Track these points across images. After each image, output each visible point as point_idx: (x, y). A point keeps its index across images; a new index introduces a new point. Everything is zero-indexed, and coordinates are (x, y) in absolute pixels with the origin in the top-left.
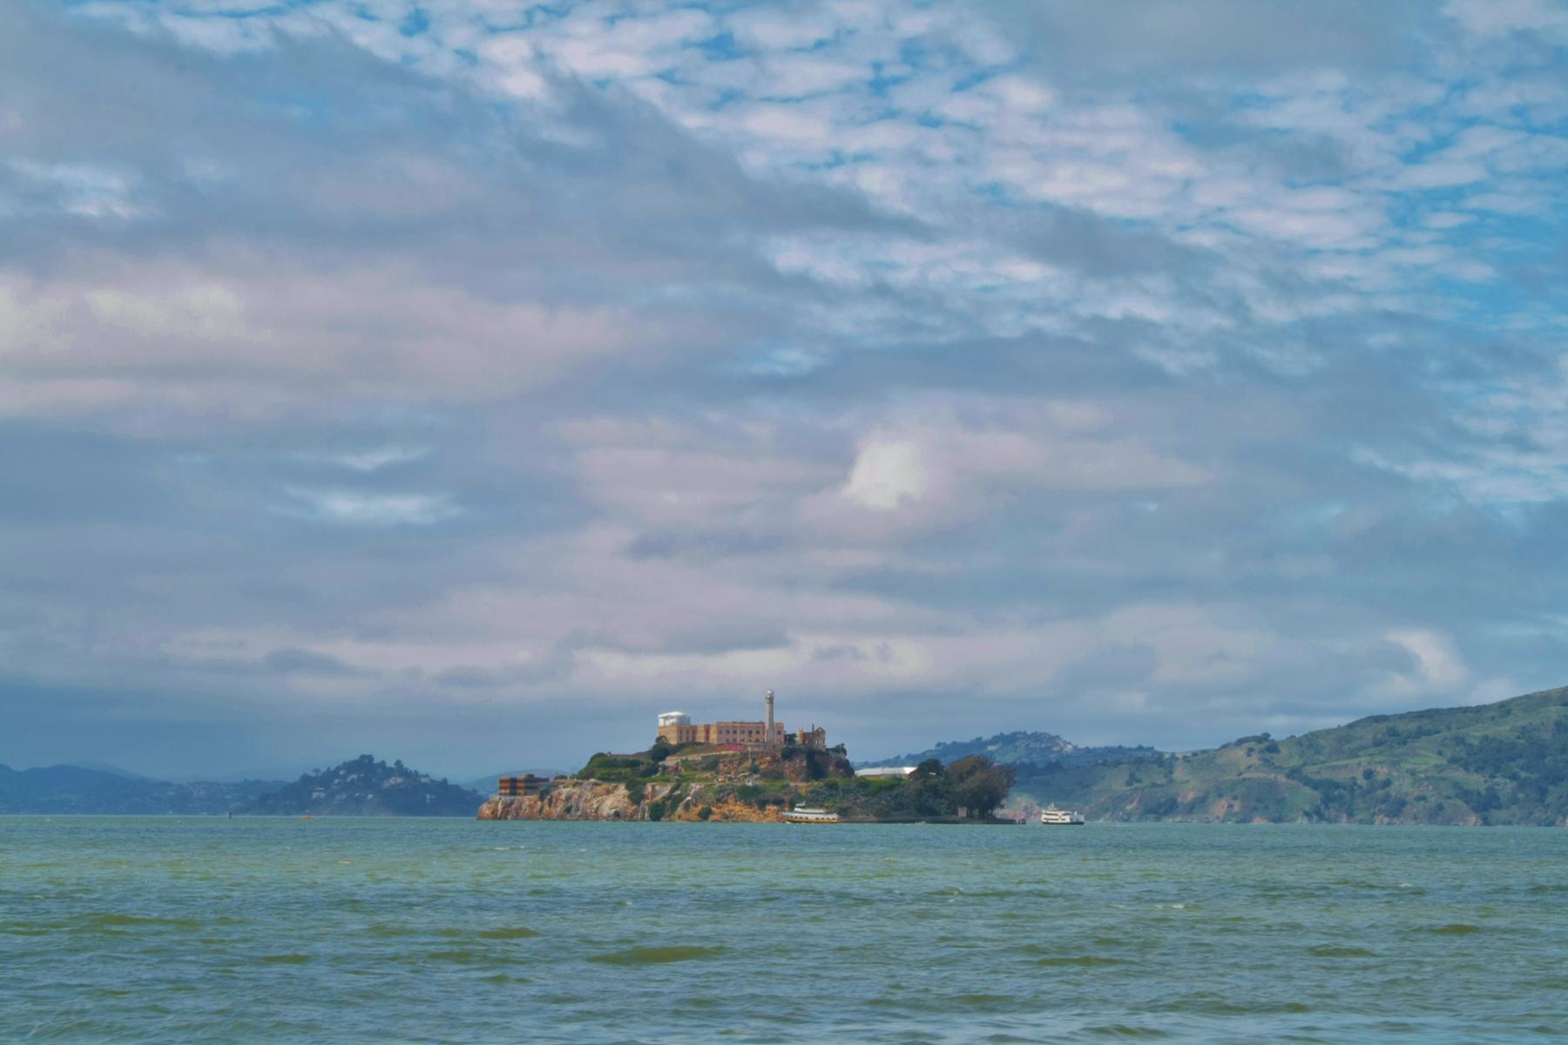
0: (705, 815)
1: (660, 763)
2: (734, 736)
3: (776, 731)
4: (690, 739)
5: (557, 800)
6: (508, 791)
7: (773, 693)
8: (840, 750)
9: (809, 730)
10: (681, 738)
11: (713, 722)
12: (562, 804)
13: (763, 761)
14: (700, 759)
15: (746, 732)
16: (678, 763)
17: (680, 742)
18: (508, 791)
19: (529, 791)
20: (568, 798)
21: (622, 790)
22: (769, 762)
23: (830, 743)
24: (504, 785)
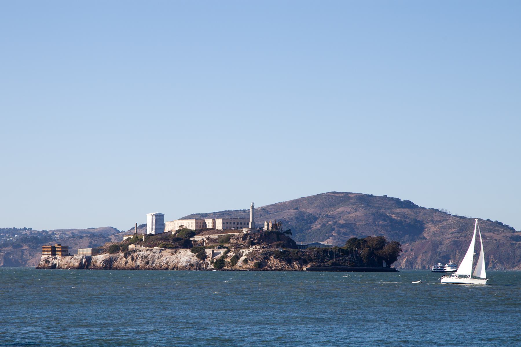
1: (191, 239)
5: (137, 258)
6: (50, 253)
10: (197, 226)
12: (141, 259)
17: (197, 228)
18: (50, 253)
19: (63, 253)
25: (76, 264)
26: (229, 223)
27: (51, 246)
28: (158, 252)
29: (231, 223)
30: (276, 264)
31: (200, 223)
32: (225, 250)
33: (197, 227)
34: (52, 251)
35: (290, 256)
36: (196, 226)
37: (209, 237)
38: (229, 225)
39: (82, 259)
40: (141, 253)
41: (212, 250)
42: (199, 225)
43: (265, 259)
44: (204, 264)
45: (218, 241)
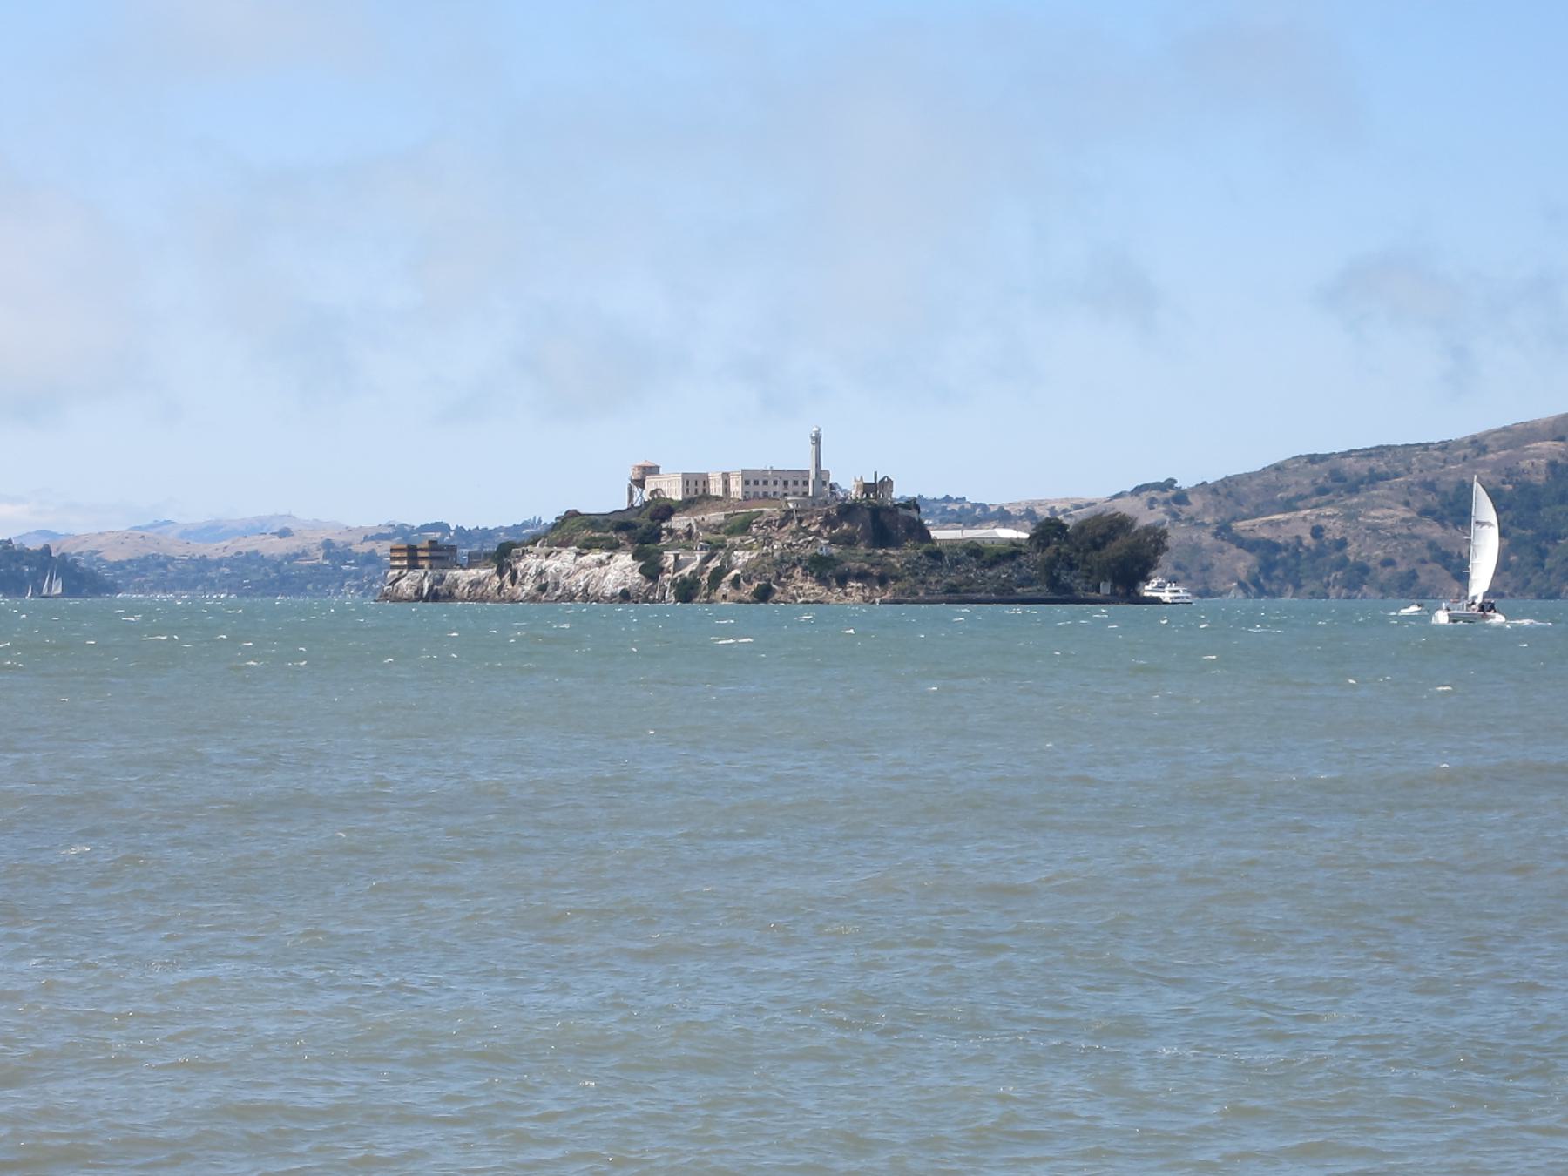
0: (763, 595)
1: (664, 525)
2: (765, 489)
4: (700, 492)
5: (524, 576)
6: (405, 563)
7: (820, 430)
10: (688, 490)
11: (735, 468)
13: (813, 521)
14: (723, 518)
15: (780, 483)
16: (690, 524)
17: (687, 497)
18: (405, 563)
19: (435, 563)
20: (541, 573)
21: (624, 560)
22: (821, 524)
24: (398, 555)
26: (761, 483)
27: (405, 546)
32: (705, 553)
34: (409, 558)
37: (703, 519)
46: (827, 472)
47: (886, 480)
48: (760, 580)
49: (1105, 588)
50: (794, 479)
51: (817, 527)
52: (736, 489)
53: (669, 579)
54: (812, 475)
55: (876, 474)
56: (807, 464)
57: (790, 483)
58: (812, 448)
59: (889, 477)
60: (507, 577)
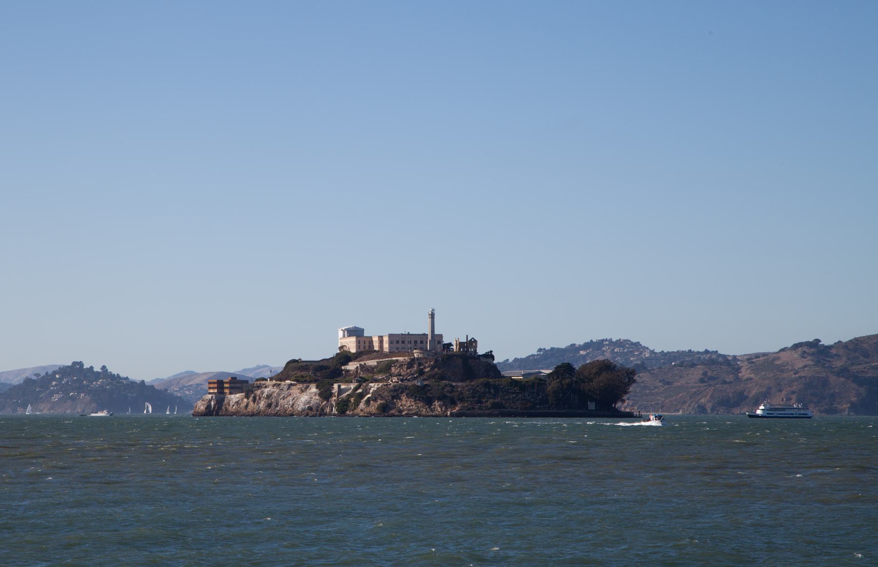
1: (343, 368)
3: (437, 342)
5: (260, 399)
6: (216, 391)
8: (490, 356)
9: (464, 340)
10: (359, 346)
14: (376, 364)
15: (413, 342)
16: (358, 367)
17: (359, 350)
18: (216, 391)
19: (232, 390)
21: (313, 389)
22: (432, 366)
23: (481, 350)
24: (212, 386)
25: (202, 407)
26: (400, 342)
27: (216, 381)
28: (286, 388)
29: (403, 342)
30: (409, 406)
31: (365, 342)
33: (359, 348)
35: (431, 394)
36: (358, 347)
37: (365, 364)
38: (400, 345)
39: (210, 401)
40: (266, 390)
41: (338, 385)
42: (362, 344)
43: (393, 397)
44: (327, 407)
45: (375, 370)
46: (441, 336)
47: (473, 340)
48: (382, 400)
49: (592, 406)
50: (418, 340)
51: (429, 369)
52: (386, 346)
53: (335, 400)
54: (430, 338)
55: (467, 336)
56: (428, 332)
57: (419, 342)
58: (429, 320)
59: (475, 338)
60: (251, 399)
